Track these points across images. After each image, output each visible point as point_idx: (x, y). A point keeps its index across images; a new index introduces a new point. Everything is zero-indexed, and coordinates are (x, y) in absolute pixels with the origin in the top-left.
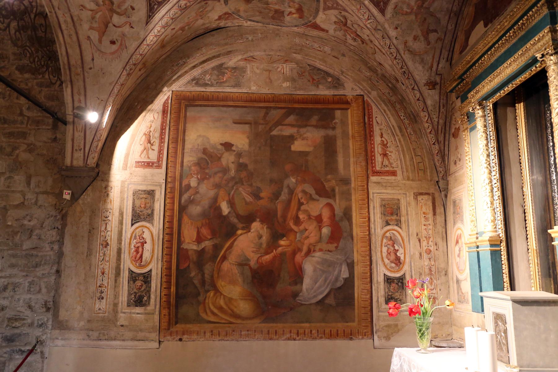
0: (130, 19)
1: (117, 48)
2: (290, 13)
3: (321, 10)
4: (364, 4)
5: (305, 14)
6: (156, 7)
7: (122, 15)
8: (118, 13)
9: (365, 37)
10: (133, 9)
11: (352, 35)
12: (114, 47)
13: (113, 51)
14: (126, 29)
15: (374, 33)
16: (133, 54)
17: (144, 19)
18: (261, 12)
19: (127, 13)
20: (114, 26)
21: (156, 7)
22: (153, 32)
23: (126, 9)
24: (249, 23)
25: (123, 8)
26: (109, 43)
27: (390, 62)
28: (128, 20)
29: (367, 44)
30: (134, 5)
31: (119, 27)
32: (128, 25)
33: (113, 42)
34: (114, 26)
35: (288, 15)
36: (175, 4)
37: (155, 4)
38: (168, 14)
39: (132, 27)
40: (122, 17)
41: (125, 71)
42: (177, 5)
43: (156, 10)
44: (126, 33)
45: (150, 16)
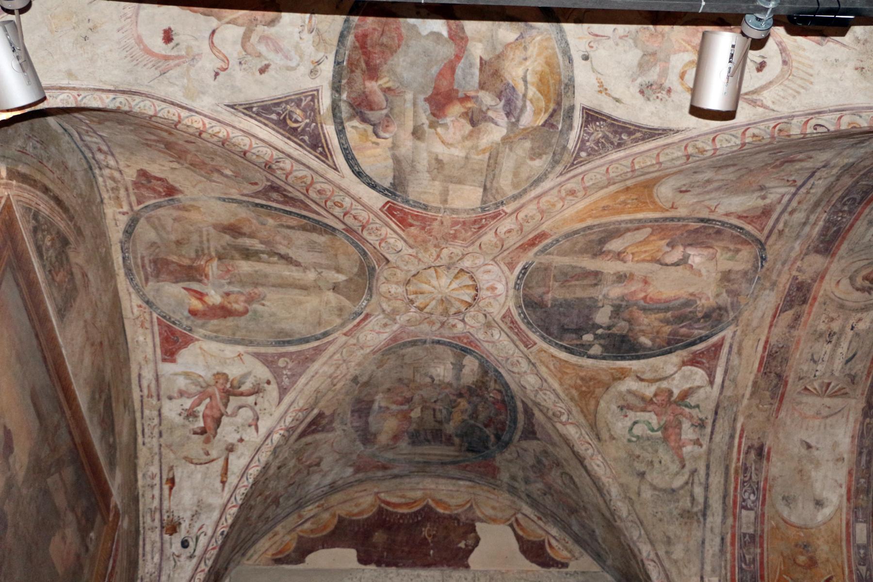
0: (237, 67)
1: (156, 50)
2: (200, 296)
3: (251, 349)
4: (313, 410)
5: (215, 322)
6: (274, 116)
7: (243, 46)
8: (246, 37)
9: (227, 432)
10: (262, 71)
11: (201, 409)
12: (157, 44)
13: (147, 41)
14: (209, 63)
15: (264, 449)
16: (153, 97)
17: (240, 98)
18: (178, 243)
19: (249, 58)
20: (213, 32)
21: (274, 116)
22: (214, 123)
23: (259, 55)
24: (123, 220)
25: (262, 48)
26: (166, 27)
27: (217, 501)
28: (233, 62)
29: (207, 441)
30: (271, 72)
31: (212, 44)
32: (220, 64)
33: (168, 36)
34: (213, 32)
35: (185, 288)
36: (283, 152)
37: (279, 114)
38: (261, 144)
39: (217, 74)
40: (239, 47)
41: (111, 96)
42: (281, 155)
43: (268, 119)
44: (200, 64)
45: (249, 108)
